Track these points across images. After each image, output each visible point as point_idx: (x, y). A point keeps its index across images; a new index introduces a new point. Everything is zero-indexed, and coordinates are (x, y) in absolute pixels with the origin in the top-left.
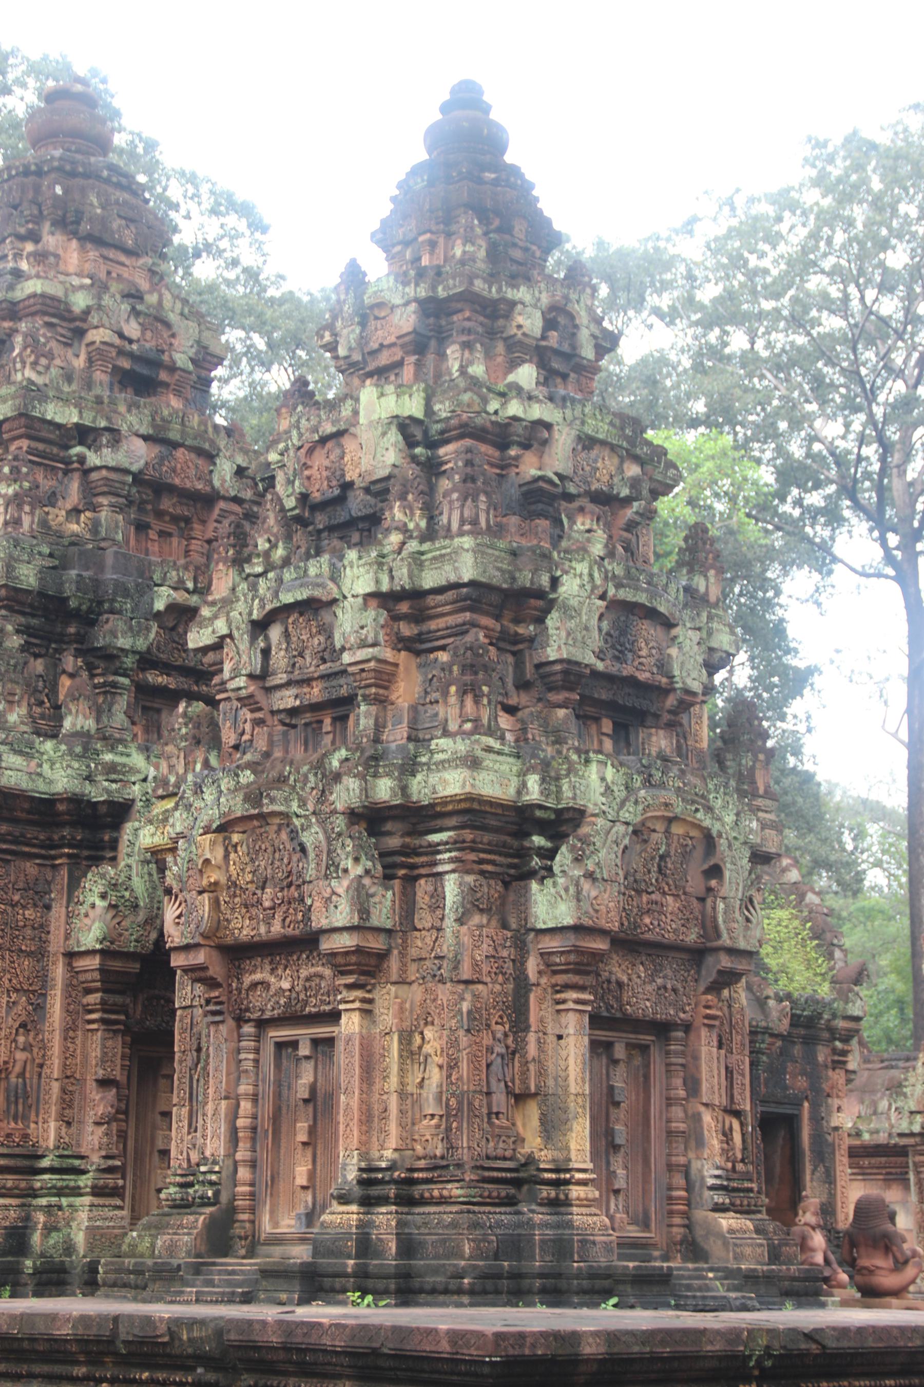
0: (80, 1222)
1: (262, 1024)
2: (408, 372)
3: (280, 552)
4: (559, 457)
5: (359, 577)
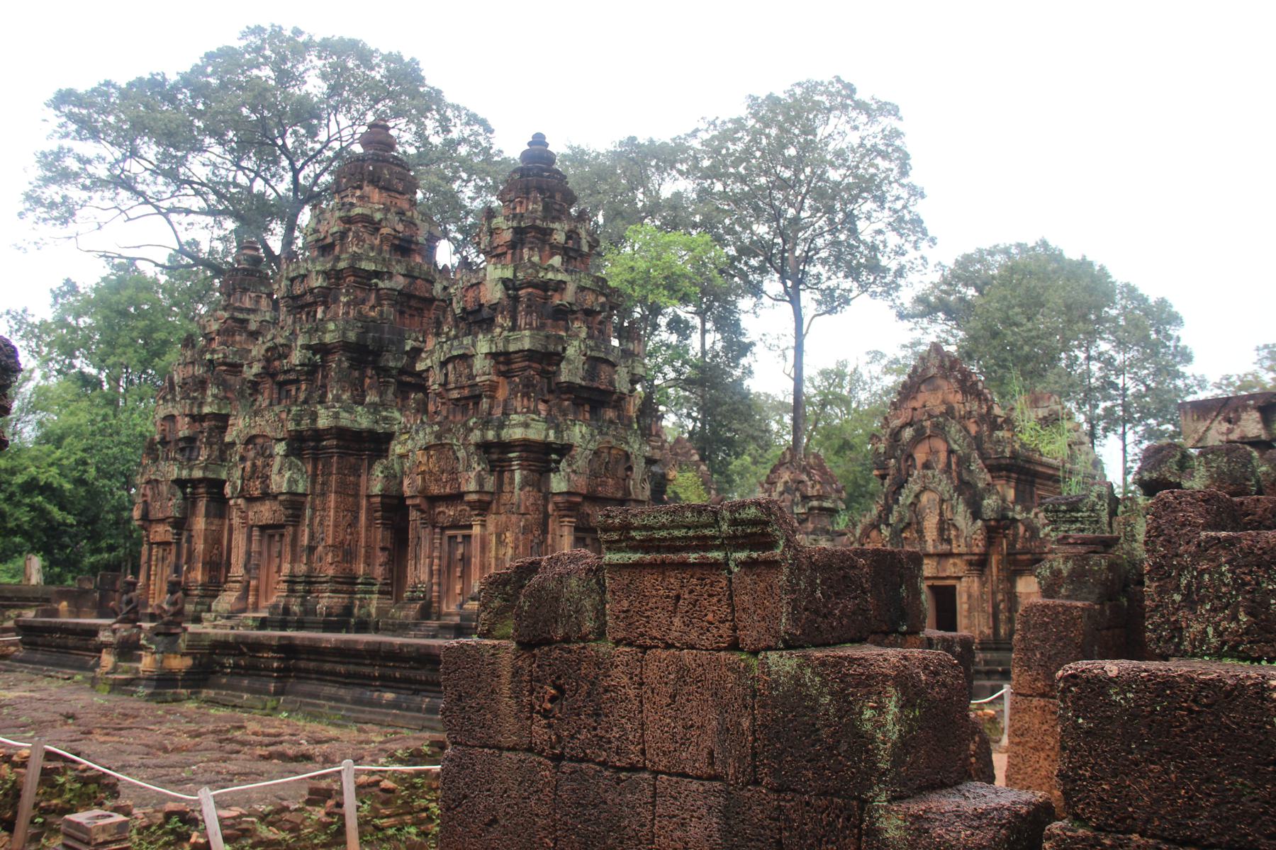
0: (374, 604)
1: (443, 529)
2: (509, 256)
3: (453, 333)
4: (569, 295)
5: (483, 346)
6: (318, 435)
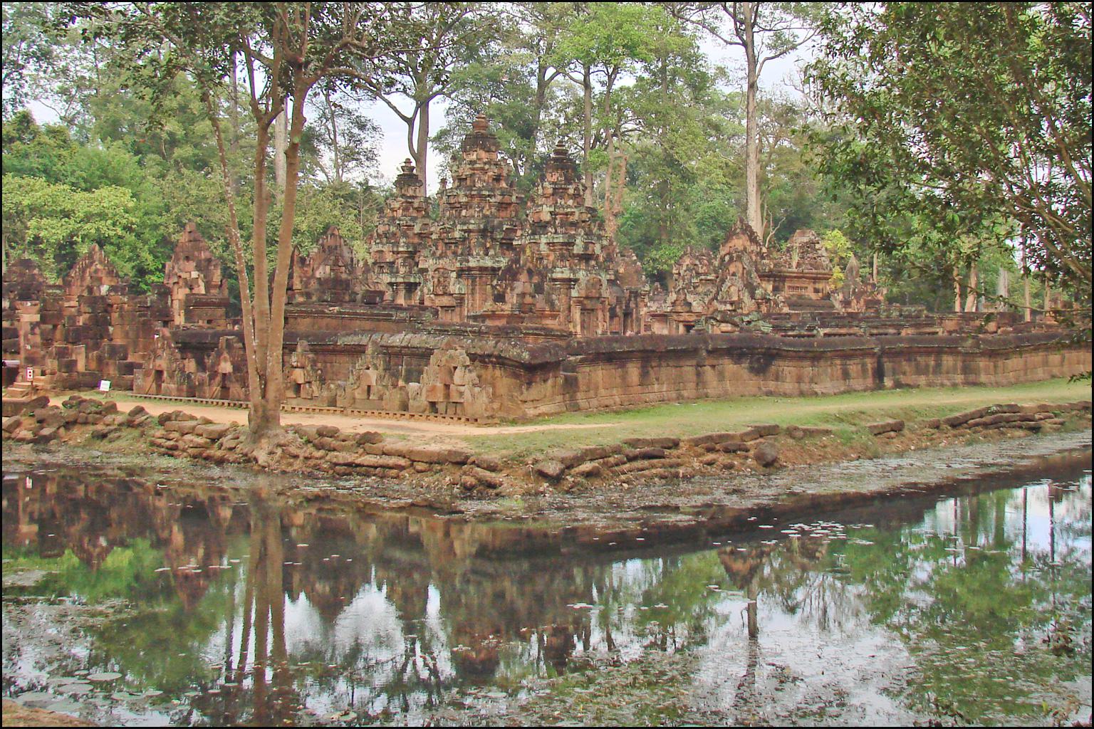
4: (576, 218)
6: (470, 269)
